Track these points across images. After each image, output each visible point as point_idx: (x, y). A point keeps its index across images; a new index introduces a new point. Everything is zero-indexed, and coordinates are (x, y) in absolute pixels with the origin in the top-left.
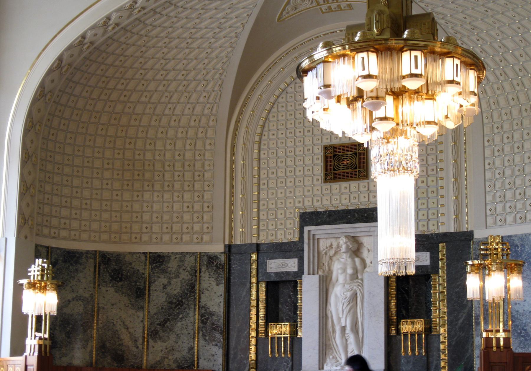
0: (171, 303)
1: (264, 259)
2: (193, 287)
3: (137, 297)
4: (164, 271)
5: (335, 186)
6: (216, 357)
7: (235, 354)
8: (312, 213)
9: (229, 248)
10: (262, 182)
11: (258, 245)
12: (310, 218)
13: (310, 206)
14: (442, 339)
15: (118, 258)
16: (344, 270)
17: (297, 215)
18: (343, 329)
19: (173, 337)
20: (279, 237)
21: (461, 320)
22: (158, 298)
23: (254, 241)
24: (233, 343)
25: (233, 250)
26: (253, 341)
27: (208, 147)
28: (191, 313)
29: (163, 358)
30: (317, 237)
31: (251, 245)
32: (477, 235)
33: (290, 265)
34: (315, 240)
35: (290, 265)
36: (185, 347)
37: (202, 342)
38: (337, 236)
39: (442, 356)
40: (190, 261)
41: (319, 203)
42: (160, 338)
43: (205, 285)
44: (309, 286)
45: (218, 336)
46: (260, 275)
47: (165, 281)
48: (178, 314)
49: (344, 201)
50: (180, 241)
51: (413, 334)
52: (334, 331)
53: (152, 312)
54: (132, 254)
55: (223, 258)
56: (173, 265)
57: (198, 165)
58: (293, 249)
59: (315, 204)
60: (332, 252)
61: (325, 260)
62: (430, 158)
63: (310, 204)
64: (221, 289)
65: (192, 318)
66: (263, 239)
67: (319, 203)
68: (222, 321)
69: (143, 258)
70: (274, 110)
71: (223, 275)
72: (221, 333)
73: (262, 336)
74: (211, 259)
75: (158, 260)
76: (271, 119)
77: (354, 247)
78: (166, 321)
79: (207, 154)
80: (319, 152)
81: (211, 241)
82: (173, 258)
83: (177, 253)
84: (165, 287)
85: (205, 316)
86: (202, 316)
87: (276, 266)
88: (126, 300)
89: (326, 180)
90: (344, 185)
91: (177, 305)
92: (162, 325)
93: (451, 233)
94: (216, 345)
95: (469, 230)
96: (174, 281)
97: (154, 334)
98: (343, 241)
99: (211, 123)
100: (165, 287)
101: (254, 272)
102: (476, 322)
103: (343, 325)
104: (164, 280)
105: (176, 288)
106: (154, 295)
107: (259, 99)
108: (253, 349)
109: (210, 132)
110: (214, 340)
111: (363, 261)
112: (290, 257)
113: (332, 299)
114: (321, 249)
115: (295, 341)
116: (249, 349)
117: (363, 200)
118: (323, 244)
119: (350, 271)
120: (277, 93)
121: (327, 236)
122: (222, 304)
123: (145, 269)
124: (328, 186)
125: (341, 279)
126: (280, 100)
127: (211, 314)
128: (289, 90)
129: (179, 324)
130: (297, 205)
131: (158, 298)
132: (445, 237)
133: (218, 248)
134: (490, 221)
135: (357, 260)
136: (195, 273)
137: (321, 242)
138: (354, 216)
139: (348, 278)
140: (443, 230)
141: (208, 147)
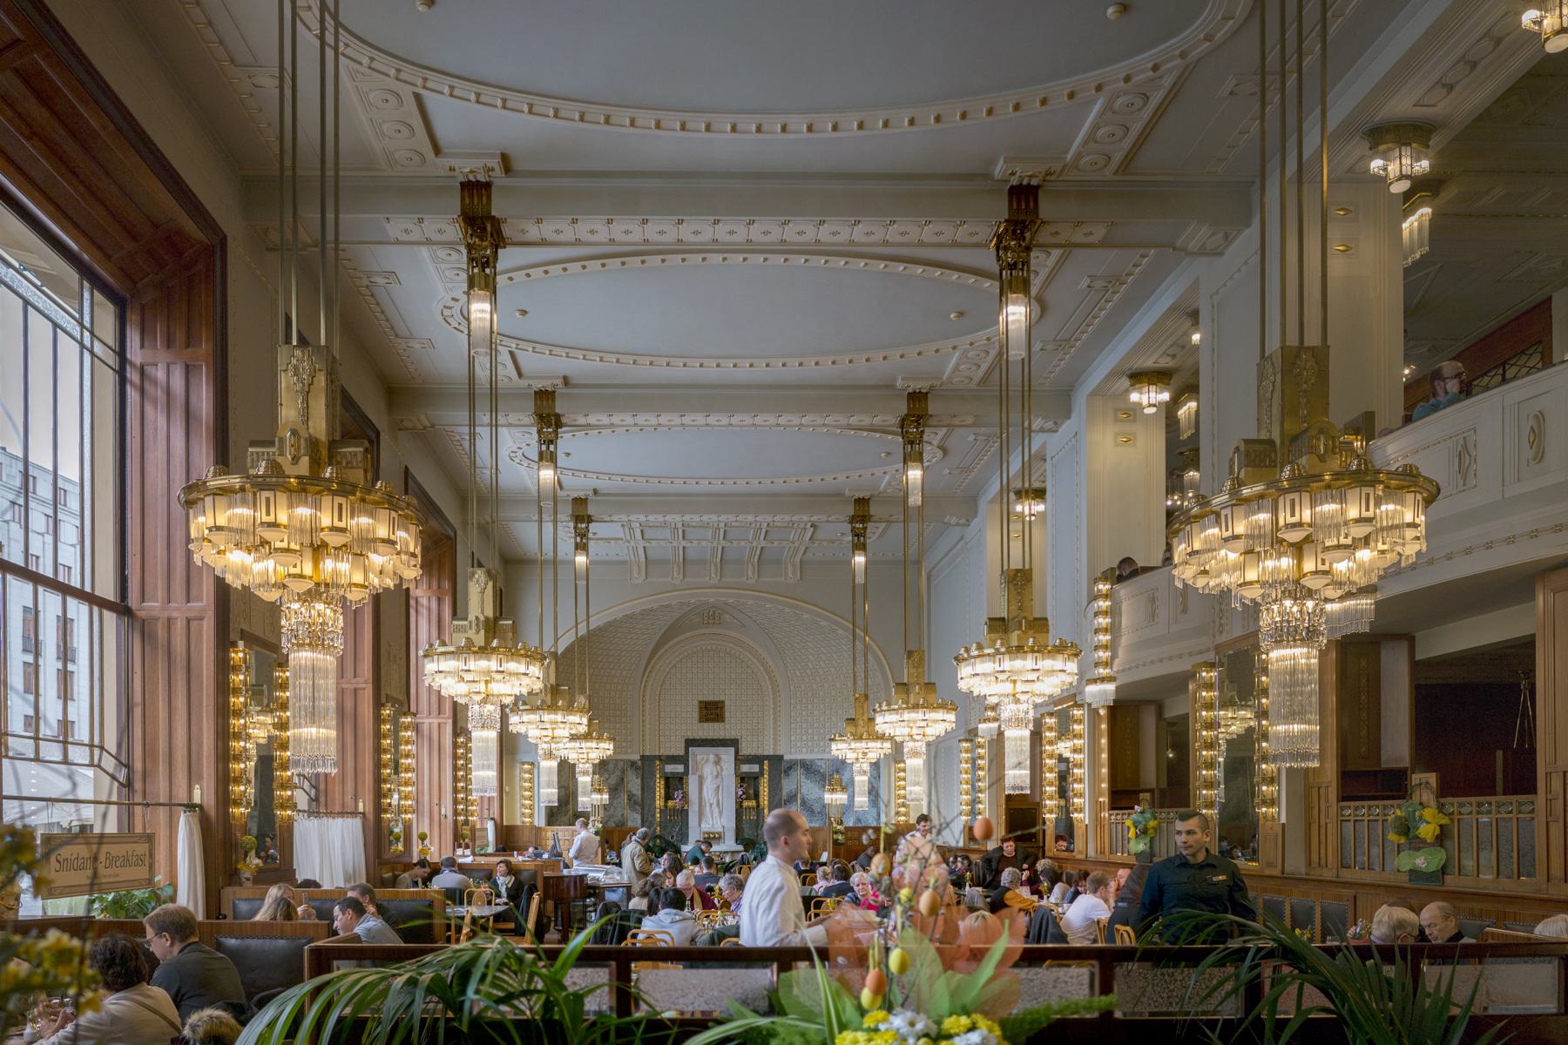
5: (706, 725)
12: (690, 743)
32: (786, 757)
33: (680, 768)
35: (680, 768)
44: (692, 782)
56: (611, 766)
66: (664, 752)
74: (633, 764)
80: (696, 703)
87: (670, 768)
115: (683, 814)
118: (699, 758)
133: (636, 757)
136: (623, 771)
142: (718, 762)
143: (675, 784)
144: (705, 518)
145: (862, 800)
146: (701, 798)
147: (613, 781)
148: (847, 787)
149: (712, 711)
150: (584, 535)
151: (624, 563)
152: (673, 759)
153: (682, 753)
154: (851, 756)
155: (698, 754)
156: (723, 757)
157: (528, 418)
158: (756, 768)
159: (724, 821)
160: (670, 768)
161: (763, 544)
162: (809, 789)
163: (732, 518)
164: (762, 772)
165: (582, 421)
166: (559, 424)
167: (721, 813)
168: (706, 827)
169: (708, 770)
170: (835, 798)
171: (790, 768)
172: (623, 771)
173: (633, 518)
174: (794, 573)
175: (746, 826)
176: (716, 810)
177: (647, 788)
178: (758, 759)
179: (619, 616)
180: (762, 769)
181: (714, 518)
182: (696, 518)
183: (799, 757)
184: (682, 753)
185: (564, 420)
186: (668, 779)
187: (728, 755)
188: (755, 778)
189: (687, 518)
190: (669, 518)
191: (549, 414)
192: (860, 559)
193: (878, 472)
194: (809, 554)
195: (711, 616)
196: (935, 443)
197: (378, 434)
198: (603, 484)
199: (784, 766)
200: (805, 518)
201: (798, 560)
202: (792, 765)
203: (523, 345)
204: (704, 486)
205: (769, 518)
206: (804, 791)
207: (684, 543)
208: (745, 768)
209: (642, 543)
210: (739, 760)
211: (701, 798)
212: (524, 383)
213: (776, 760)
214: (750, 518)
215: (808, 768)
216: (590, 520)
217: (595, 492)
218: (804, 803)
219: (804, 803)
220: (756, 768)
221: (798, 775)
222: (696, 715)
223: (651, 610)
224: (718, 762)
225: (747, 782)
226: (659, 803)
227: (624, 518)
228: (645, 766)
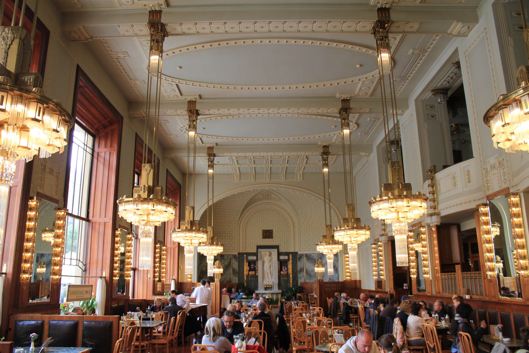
2: (230, 263)
4: (224, 259)
5: (265, 240)
9: (239, 253)
12: (259, 247)
32: (299, 253)
33: (254, 258)
34: (261, 252)
35: (254, 258)
40: (229, 257)
44: (260, 263)
56: (226, 257)
58: (256, 254)
64: (237, 263)
66: (247, 251)
74: (235, 256)
80: (261, 231)
87: (250, 258)
90: (267, 239)
98: (268, 253)
113: (265, 266)
115: (256, 277)
118: (262, 253)
125: (267, 262)
133: (236, 253)
136: (230, 259)
142: (270, 255)
143: (253, 266)
144: (262, 154)
145: (331, 270)
147: (226, 263)
148: (324, 265)
149: (268, 234)
150: (212, 162)
151: (231, 174)
153: (255, 251)
154: (325, 252)
155: (262, 251)
156: (272, 253)
157: (186, 113)
159: (273, 280)
160: (250, 258)
161: (287, 165)
163: (273, 154)
164: (289, 260)
165: (207, 112)
166: (198, 114)
167: (272, 277)
168: (265, 283)
169: (266, 259)
170: (319, 270)
171: (300, 257)
172: (230, 259)
173: (232, 154)
174: (300, 177)
176: (270, 275)
177: (241, 266)
178: (287, 254)
179: (229, 195)
180: (289, 258)
181: (265, 154)
182: (258, 154)
183: (304, 253)
184: (255, 251)
185: (200, 112)
186: (250, 263)
187: (275, 252)
189: (254, 154)
190: (247, 154)
191: (193, 111)
192: (326, 170)
193: (332, 134)
194: (306, 170)
195: (266, 195)
196: (354, 121)
197: (122, 118)
198: (219, 141)
199: (298, 256)
200: (303, 153)
201: (301, 172)
202: (301, 256)
203: (181, 81)
204: (261, 141)
205: (288, 154)
207: (254, 166)
208: (282, 258)
209: (238, 166)
210: (279, 254)
212: (182, 98)
213: (295, 254)
214: (280, 154)
216: (214, 156)
217: (217, 144)
219: (307, 272)
221: (304, 259)
222: (261, 236)
223: (242, 193)
224: (270, 255)
225: (282, 264)
226: (246, 273)
227: (228, 154)
228: (240, 257)
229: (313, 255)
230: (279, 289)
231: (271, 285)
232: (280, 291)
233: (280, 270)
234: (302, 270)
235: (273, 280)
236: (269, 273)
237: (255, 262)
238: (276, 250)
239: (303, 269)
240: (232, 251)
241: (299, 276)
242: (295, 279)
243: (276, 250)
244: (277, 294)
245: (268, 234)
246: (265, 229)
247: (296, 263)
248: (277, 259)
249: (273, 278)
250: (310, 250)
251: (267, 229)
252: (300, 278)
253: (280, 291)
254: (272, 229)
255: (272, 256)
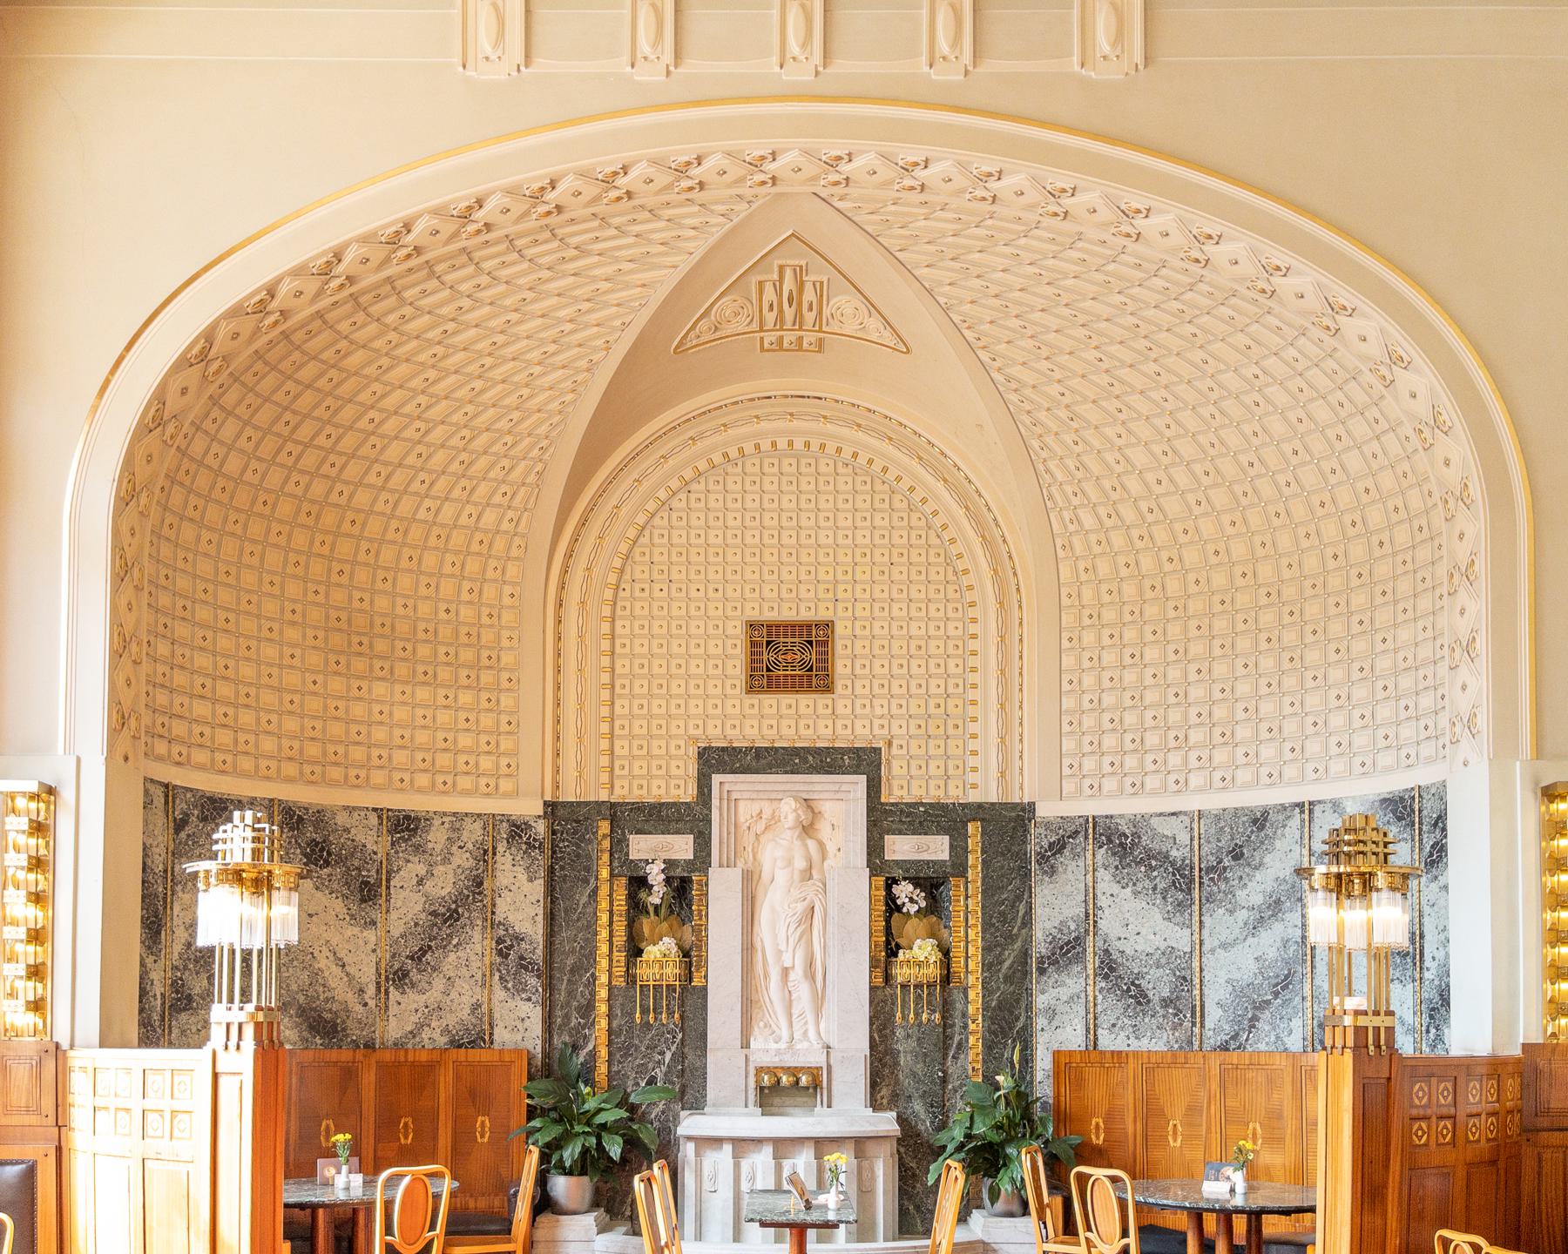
0: (434, 914)
1: (623, 834)
3: (363, 901)
4: (418, 849)
5: (769, 701)
6: (527, 1022)
7: (567, 1017)
8: (723, 749)
10: (618, 683)
11: (613, 805)
12: (717, 760)
13: (718, 735)
14: (972, 995)
15: (320, 817)
16: (789, 863)
17: (693, 752)
18: (785, 972)
19: (439, 983)
20: (655, 791)
21: (1007, 964)
22: (406, 905)
23: (604, 796)
24: (561, 997)
25: (561, 812)
26: (603, 993)
27: (507, 601)
28: (477, 936)
29: (421, 1026)
30: (734, 796)
31: (599, 804)
32: (1045, 811)
33: (681, 847)
35: (681, 847)
36: (467, 1001)
37: (499, 994)
38: (773, 796)
39: (972, 1027)
41: (737, 731)
42: (413, 985)
43: (503, 879)
44: (721, 892)
45: (533, 981)
46: (616, 864)
47: (422, 870)
48: (450, 936)
49: (785, 731)
50: (449, 790)
51: (918, 986)
52: (766, 976)
53: (396, 933)
54: (350, 810)
55: (541, 828)
56: (437, 837)
57: (487, 636)
59: (729, 732)
60: (760, 827)
61: (748, 840)
62: (951, 663)
63: (718, 731)
65: (476, 947)
67: (737, 731)
68: (539, 952)
69: (373, 819)
70: (644, 540)
71: (542, 860)
72: (538, 977)
73: (620, 982)
74: (517, 829)
75: (405, 826)
76: (638, 558)
77: (804, 817)
78: (424, 951)
79: (507, 617)
80: (737, 631)
81: (516, 794)
82: (437, 822)
83: (445, 814)
84: (420, 882)
85: (506, 945)
86: (499, 941)
88: (338, 906)
89: (751, 689)
90: (787, 699)
91: (447, 918)
92: (417, 957)
93: (993, 804)
94: (529, 999)
95: (1026, 801)
96: (439, 870)
97: (400, 978)
98: (789, 810)
99: (514, 552)
100: (420, 882)
101: (606, 857)
102: (1038, 969)
103: (788, 964)
104: (417, 868)
105: (444, 884)
106: (398, 897)
107: (613, 515)
108: (603, 1008)
109: (512, 571)
110: (524, 990)
111: (821, 845)
112: (677, 832)
114: (742, 819)
115: (689, 997)
116: (594, 1008)
117: (822, 731)
118: (745, 811)
119: (800, 864)
120: (651, 506)
121: (754, 796)
122: (540, 918)
123: (374, 841)
124: (755, 699)
125: (782, 877)
126: (657, 521)
127: (519, 938)
128: (675, 503)
129: (452, 956)
130: (692, 732)
131: (406, 905)
132: (980, 811)
133: (529, 808)
134: (1068, 787)
135: (811, 844)
136: (485, 855)
137: (741, 804)
138: (805, 760)
139: (797, 876)
140: (974, 797)
141: (507, 601)
146: (749, 948)
152: (658, 817)
153: (686, 792)
156: (829, 809)
158: (937, 848)
159: (830, 1028)
162: (1137, 924)
164: (959, 866)
167: (819, 1001)
168: (769, 1049)
169: (778, 857)
171: (1058, 847)
172: (485, 855)
175: (905, 1048)
176: (802, 992)
184: (686, 792)
187: (843, 800)
188: (932, 883)
199: (1037, 840)
206: (1109, 924)
208: (901, 848)
210: (883, 818)
211: (749, 948)
213: (1008, 825)
215: (1122, 844)
218: (1108, 967)
220: (937, 848)
222: (737, 669)
225: (907, 898)
226: (606, 969)
229: (1166, 827)
230: (875, 1105)
231: (814, 1073)
232: (887, 1123)
233: (889, 949)
234: (1067, 951)
235: (830, 1028)
236: (797, 975)
237: (683, 889)
238: (857, 785)
239: (1078, 941)
240: (493, 792)
241: (1041, 1001)
242: (1009, 1023)
243: (857, 785)
244: (860, 1144)
245: (790, 655)
246: (770, 616)
247: (1024, 893)
248: (861, 858)
249: (831, 1007)
250: (1138, 789)
251: (787, 614)
252: (1052, 1013)
253: (887, 1123)
254: (823, 615)
255: (824, 830)
